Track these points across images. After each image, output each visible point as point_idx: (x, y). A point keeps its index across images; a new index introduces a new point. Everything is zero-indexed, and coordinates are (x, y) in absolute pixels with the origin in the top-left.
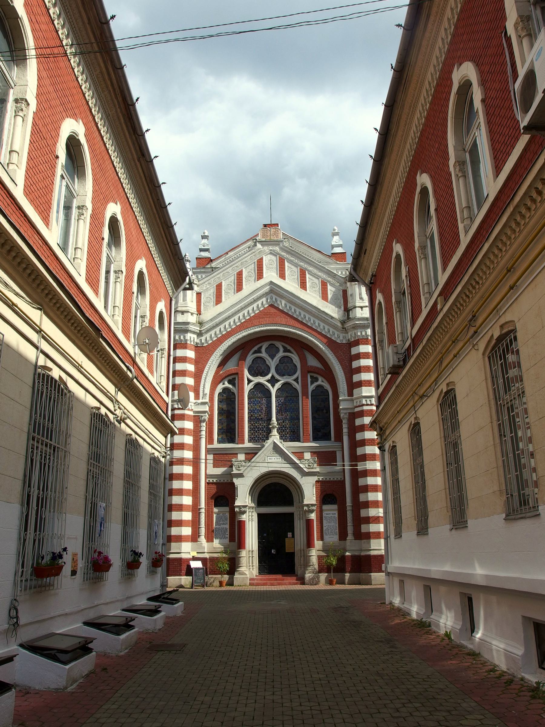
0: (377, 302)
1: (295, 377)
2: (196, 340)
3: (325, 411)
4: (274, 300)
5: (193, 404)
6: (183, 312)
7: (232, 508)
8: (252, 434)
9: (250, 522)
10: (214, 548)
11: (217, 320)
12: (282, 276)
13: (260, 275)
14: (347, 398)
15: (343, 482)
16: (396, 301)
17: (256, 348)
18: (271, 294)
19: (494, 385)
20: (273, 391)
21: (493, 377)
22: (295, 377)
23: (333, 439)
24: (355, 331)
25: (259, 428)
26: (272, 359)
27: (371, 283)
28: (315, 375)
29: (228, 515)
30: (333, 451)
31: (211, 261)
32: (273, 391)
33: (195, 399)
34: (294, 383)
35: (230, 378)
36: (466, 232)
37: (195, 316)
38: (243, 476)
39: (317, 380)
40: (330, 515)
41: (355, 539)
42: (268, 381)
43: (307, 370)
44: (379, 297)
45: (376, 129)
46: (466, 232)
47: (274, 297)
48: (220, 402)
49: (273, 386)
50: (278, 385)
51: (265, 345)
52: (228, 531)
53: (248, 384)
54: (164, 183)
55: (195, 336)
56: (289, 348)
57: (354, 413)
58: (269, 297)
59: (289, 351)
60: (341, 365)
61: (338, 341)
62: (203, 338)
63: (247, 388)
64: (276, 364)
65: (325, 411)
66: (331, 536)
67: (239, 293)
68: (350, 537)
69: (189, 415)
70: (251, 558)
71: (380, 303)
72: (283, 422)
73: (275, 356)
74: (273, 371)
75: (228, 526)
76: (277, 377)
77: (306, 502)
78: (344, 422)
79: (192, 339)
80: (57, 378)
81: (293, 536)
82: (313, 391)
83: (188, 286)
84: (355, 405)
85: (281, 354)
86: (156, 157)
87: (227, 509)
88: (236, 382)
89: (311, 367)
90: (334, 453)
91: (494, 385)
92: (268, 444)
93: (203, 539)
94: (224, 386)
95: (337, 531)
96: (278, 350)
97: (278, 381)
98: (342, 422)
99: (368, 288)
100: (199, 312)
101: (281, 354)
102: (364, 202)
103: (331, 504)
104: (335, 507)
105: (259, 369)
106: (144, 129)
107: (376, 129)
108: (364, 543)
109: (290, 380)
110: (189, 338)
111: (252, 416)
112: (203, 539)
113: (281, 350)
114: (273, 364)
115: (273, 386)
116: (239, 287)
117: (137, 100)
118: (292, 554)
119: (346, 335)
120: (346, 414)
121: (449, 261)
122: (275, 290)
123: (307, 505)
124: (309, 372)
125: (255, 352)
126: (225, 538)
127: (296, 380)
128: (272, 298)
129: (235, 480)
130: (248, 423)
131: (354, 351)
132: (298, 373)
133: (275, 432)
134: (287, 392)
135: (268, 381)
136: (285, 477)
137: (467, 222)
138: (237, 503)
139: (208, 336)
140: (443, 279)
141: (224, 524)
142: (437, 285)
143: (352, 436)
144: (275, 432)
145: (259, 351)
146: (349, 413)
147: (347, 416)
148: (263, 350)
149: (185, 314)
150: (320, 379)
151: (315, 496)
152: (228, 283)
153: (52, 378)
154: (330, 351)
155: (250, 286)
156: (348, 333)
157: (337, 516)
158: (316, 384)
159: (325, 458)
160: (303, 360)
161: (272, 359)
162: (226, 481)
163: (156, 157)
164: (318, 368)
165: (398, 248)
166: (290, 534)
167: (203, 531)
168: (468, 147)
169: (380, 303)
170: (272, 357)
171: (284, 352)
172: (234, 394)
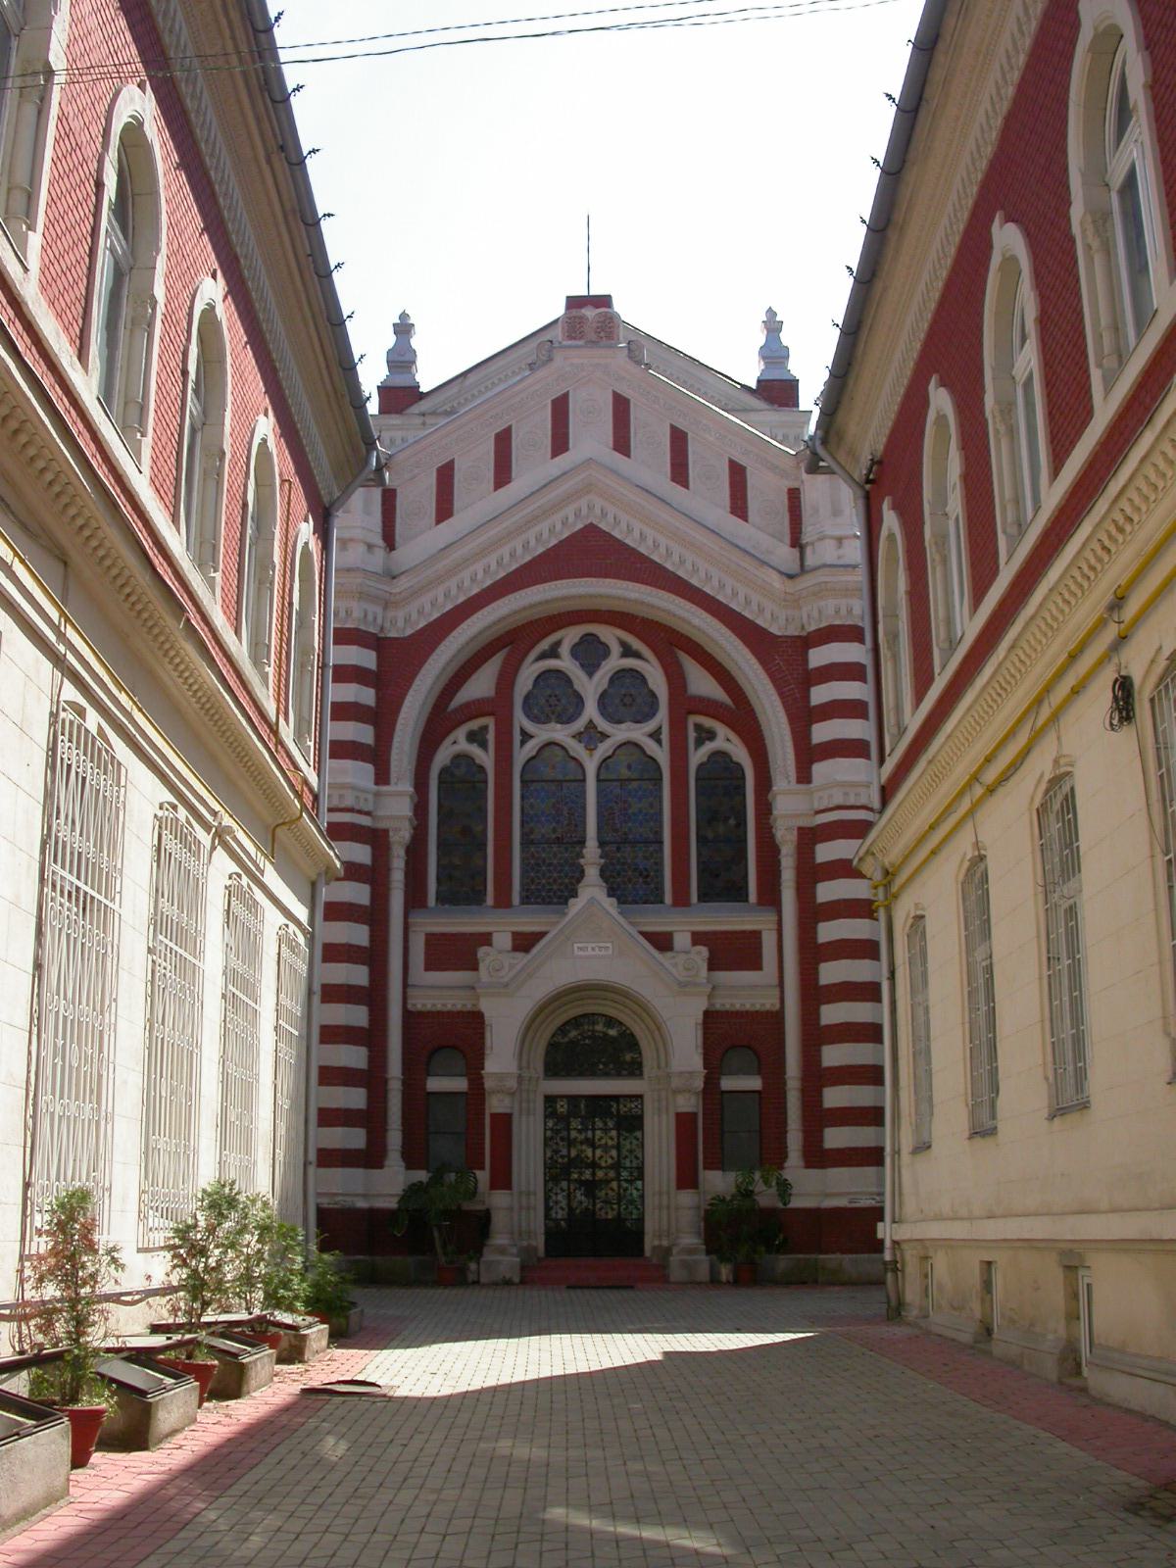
0: (884, 533)
2: (379, 621)
3: (732, 822)
4: (598, 511)
5: (370, 797)
8: (533, 881)
9: (524, 1118)
12: (622, 445)
13: (560, 443)
15: (777, 1018)
16: (934, 535)
17: (545, 645)
19: (1160, 767)
21: (1158, 749)
22: (650, 726)
23: (753, 897)
24: (823, 603)
26: (590, 675)
27: (868, 481)
28: (708, 722)
31: (423, 396)
33: (377, 783)
36: (1108, 390)
37: (380, 554)
39: (711, 735)
42: (578, 736)
43: (684, 705)
44: (890, 521)
45: (889, 97)
46: (1108, 390)
47: (599, 503)
49: (591, 750)
50: (604, 749)
51: (571, 636)
54: (329, 215)
55: (379, 610)
56: (636, 644)
58: (583, 503)
59: (637, 655)
60: (781, 694)
61: (775, 630)
62: (401, 614)
64: (600, 690)
65: (732, 822)
67: (502, 491)
70: (524, 1213)
71: (891, 537)
72: (618, 849)
73: (597, 666)
74: (591, 711)
76: (603, 725)
79: (370, 618)
80: (94, 731)
82: (701, 767)
83: (372, 476)
85: (614, 662)
86: (314, 151)
88: (491, 737)
89: (701, 700)
90: (756, 935)
91: (1160, 767)
92: (576, 905)
94: (457, 748)
96: (606, 652)
97: (604, 736)
99: (860, 493)
101: (614, 662)
102: (855, 269)
105: (553, 701)
106: (290, 87)
107: (889, 97)
109: (637, 733)
113: (616, 649)
114: (590, 688)
115: (591, 750)
116: (503, 474)
117: (277, 19)
121: (1067, 452)
124: (690, 712)
125: (543, 656)
127: (655, 736)
128: (590, 508)
129: (487, 1006)
130: (522, 851)
131: (819, 657)
132: (662, 716)
133: (592, 873)
135: (578, 736)
137: (1110, 362)
138: (491, 1066)
140: (1053, 495)
142: (1037, 508)
143: (805, 892)
144: (592, 873)
146: (799, 829)
147: (793, 837)
148: (565, 650)
150: (722, 730)
151: (700, 1050)
152: (475, 461)
153: (86, 730)
155: (533, 468)
156: (801, 608)
158: (709, 747)
159: (733, 952)
161: (590, 675)
163: (314, 151)
165: (940, 400)
167: (395, 1138)
168: (1117, 179)
169: (891, 537)
170: (590, 669)
172: (482, 769)
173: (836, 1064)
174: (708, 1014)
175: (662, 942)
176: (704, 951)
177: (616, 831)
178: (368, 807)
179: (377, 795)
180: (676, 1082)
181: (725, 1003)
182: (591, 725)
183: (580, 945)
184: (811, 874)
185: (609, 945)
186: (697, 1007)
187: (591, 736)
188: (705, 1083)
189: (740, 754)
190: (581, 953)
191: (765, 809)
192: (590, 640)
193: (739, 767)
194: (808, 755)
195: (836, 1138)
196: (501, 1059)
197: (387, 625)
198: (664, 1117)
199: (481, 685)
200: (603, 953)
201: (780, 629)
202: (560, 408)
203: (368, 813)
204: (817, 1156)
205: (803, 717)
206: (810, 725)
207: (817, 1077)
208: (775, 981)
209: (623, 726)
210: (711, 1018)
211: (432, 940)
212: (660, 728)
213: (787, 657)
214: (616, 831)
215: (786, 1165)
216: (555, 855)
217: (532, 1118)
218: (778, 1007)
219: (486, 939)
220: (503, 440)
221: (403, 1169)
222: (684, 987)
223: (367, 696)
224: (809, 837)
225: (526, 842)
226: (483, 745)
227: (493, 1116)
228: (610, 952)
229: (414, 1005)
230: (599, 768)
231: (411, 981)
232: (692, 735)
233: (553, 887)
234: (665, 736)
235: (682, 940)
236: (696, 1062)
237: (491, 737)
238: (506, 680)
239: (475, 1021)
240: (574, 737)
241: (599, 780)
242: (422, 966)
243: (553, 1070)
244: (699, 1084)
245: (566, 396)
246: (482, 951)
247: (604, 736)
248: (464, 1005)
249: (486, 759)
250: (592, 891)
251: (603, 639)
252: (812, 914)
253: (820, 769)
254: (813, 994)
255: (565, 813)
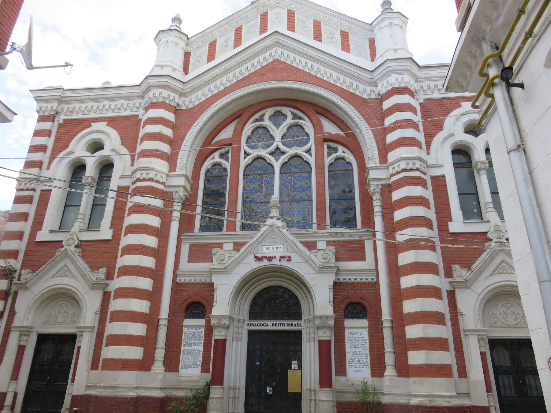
1: (306, 147)
5: (164, 176)
6: (162, 67)
7: (208, 322)
9: (234, 342)
10: (178, 381)
11: (207, 77)
12: (291, 27)
14: (378, 165)
15: (376, 285)
17: (257, 116)
18: (277, 48)
20: (277, 166)
22: (306, 147)
24: (387, 79)
25: (256, 212)
26: (278, 128)
28: (334, 145)
29: (202, 331)
30: (360, 241)
32: (277, 166)
34: (307, 155)
35: (223, 151)
38: (227, 273)
40: (357, 336)
41: (398, 376)
42: (271, 154)
47: (280, 50)
48: (208, 180)
49: (277, 160)
51: (269, 112)
52: (201, 355)
53: (245, 158)
55: (177, 97)
57: (389, 186)
58: (273, 51)
59: (300, 118)
61: (365, 96)
62: (187, 100)
63: (244, 162)
66: (358, 369)
68: (390, 371)
69: (158, 189)
70: (231, 400)
72: (290, 204)
74: (278, 143)
75: (201, 348)
76: (283, 148)
77: (317, 313)
78: (374, 198)
81: (300, 367)
82: (331, 165)
84: (391, 171)
87: (202, 322)
88: (230, 155)
90: (361, 243)
93: (158, 367)
94: (214, 160)
95: (368, 360)
97: (284, 153)
98: (372, 199)
100: (186, 71)
101: (290, 121)
103: (358, 318)
104: (364, 322)
108: (415, 382)
110: (167, 96)
111: (248, 197)
112: (158, 367)
113: (290, 116)
114: (277, 133)
115: (277, 160)
118: (298, 397)
119: (375, 88)
120: (377, 186)
122: (281, 42)
123: (320, 317)
124: (325, 140)
125: (257, 120)
126: (196, 366)
127: (308, 151)
129: (216, 280)
131: (387, 104)
132: (312, 143)
133: (274, 212)
134: (296, 167)
135: (271, 154)
136: (290, 277)
138: (215, 312)
139: (193, 97)
141: (196, 344)
143: (387, 215)
144: (274, 212)
145: (261, 119)
146: (383, 185)
147: (379, 190)
148: (266, 117)
149: (164, 68)
150: (341, 148)
151: (332, 303)
154: (353, 108)
156: (377, 86)
157: (366, 336)
158: (334, 155)
160: (318, 127)
161: (278, 128)
162: (203, 280)
164: (337, 135)
166: (295, 364)
170: (278, 125)
171: (293, 119)
172: (225, 170)
173: (413, 311)
174: (336, 284)
175: (311, 246)
176: (333, 249)
177: (289, 196)
178: (164, 180)
179: (168, 176)
180: (317, 322)
181: (345, 278)
182: (278, 148)
183: (266, 247)
184: (389, 208)
185: (282, 246)
186: (329, 279)
187: (277, 153)
188: (335, 323)
189: (350, 157)
190: (267, 251)
191: (364, 182)
192: (278, 114)
193: (350, 163)
194: (384, 150)
195: (416, 357)
196: (221, 307)
197: (181, 103)
198: (312, 343)
199: (227, 133)
200: (278, 250)
201: (368, 95)
202: (264, 18)
203: (163, 183)
204: (404, 370)
205: (381, 135)
206: (385, 137)
207: (400, 320)
208: (374, 268)
209: (293, 148)
210: (337, 286)
211: (193, 247)
212: (311, 149)
213: (373, 109)
214: (289, 196)
215: (385, 374)
216: (259, 208)
217: (240, 342)
218: (375, 280)
219: (220, 245)
220: (238, 32)
221: (163, 371)
222: (322, 270)
223: (168, 132)
224: (388, 189)
225: (244, 202)
226: (227, 160)
227: (216, 340)
228: (282, 250)
229: (180, 280)
230: (281, 168)
231: (180, 267)
232: (326, 151)
233: (253, 218)
234: (313, 152)
235: (322, 245)
236: (330, 311)
237: (230, 155)
238: (238, 132)
239: (211, 286)
240: (270, 154)
241: (281, 173)
242: (187, 259)
243: (254, 314)
244: (332, 323)
245: (266, 13)
246: (214, 251)
247: (284, 153)
248: (206, 280)
249: (227, 165)
250: (274, 221)
251: (283, 112)
252: (391, 228)
253: (392, 156)
254: (396, 272)
255: (264, 188)
